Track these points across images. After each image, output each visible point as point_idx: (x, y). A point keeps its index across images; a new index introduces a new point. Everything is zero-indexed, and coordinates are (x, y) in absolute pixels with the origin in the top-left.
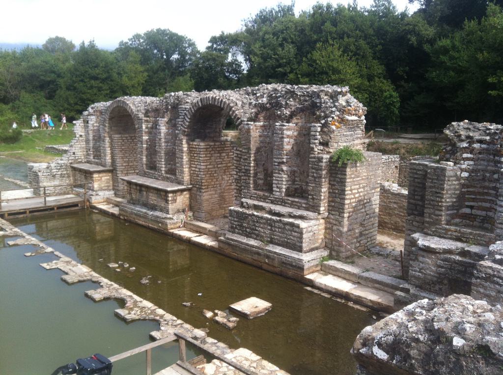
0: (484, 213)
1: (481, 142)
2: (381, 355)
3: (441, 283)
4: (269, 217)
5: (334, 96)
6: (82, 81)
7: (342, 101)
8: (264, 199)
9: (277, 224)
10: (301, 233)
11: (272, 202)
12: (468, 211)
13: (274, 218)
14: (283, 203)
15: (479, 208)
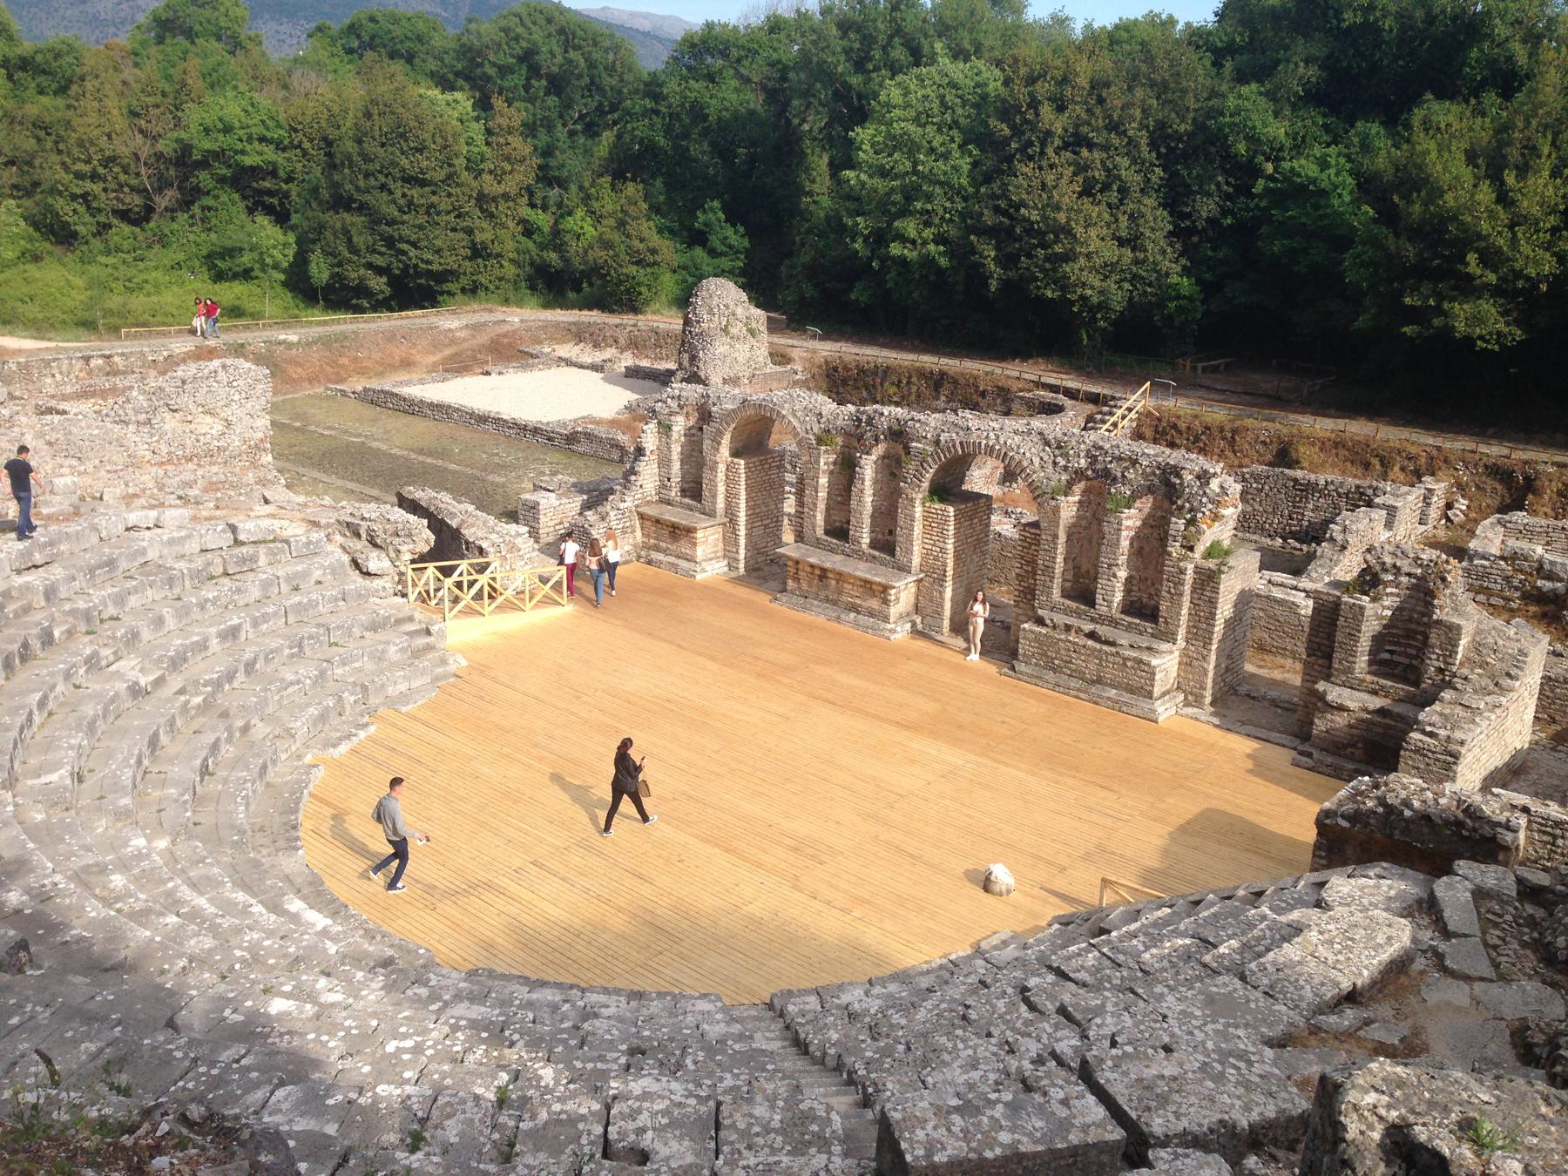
0: (1407, 661)
1: (1409, 575)
2: (1345, 824)
3: (1354, 746)
4: (1098, 646)
5: (1204, 477)
6: (383, 187)
7: (1214, 485)
8: (1079, 615)
9: (1111, 659)
10: (1154, 674)
11: (1093, 620)
12: (1386, 656)
13: (1105, 648)
14: (1113, 623)
15: (1400, 654)
